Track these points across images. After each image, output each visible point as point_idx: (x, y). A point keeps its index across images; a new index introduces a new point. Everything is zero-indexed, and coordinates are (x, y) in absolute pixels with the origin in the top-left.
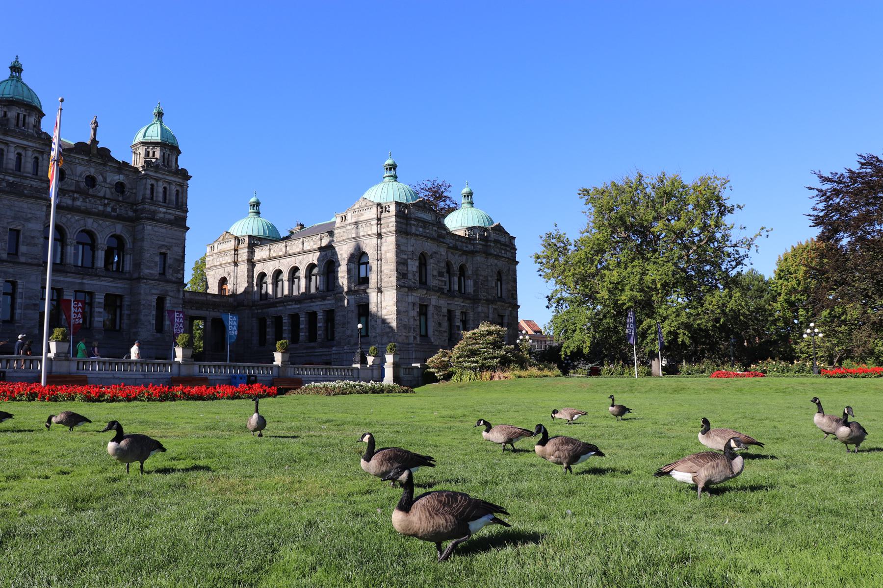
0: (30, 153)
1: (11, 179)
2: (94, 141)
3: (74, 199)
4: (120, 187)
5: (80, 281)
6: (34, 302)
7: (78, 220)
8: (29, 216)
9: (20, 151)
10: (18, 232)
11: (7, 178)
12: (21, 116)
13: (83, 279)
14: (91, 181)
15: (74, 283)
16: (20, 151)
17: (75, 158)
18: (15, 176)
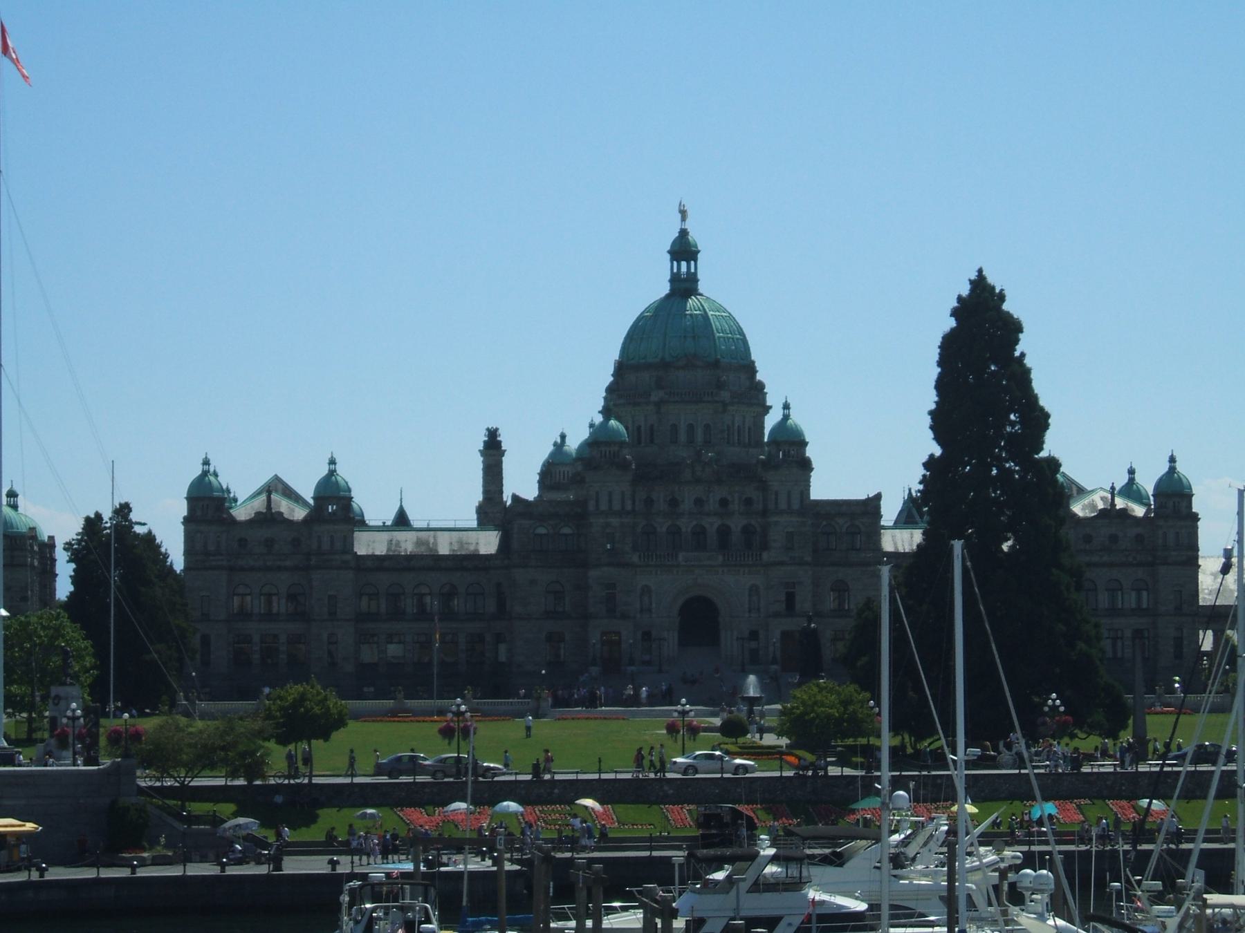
4: (1139, 538)
14: (1114, 538)
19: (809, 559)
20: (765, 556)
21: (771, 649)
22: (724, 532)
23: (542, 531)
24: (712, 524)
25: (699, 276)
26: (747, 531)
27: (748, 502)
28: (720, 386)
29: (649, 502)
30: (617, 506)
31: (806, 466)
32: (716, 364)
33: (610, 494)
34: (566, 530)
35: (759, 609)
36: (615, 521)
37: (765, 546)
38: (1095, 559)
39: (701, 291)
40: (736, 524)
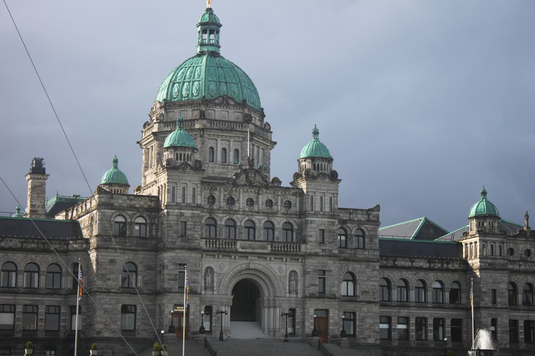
0: (497, 244)
1: (489, 261)
2: (528, 227)
3: (520, 265)
5: (526, 314)
6: (506, 329)
7: (523, 278)
8: (500, 280)
9: (492, 244)
10: (494, 291)
11: (488, 261)
12: (491, 223)
13: (528, 313)
15: (524, 316)
16: (492, 244)
17: (518, 240)
18: (491, 259)
19: (336, 252)
20: (303, 246)
21: (307, 324)
22: (270, 227)
23: (120, 219)
24: (260, 221)
25: (220, 44)
26: (288, 228)
27: (289, 204)
28: (248, 119)
29: (212, 199)
30: (189, 200)
31: (334, 177)
32: (243, 104)
33: (184, 189)
34: (141, 220)
35: (297, 293)
36: (188, 213)
37: (304, 241)
38: (517, 267)
39: (221, 55)
40: (279, 222)
